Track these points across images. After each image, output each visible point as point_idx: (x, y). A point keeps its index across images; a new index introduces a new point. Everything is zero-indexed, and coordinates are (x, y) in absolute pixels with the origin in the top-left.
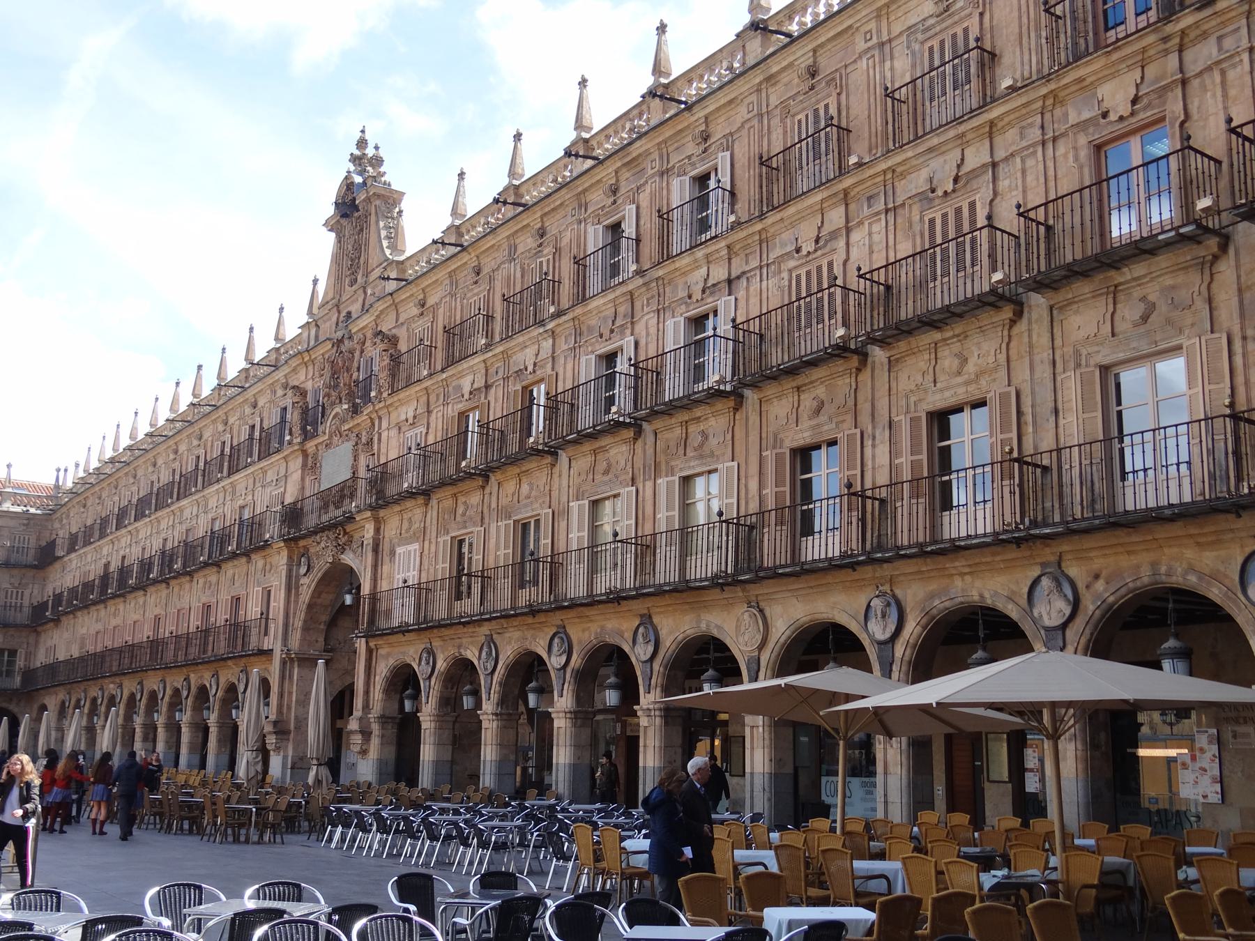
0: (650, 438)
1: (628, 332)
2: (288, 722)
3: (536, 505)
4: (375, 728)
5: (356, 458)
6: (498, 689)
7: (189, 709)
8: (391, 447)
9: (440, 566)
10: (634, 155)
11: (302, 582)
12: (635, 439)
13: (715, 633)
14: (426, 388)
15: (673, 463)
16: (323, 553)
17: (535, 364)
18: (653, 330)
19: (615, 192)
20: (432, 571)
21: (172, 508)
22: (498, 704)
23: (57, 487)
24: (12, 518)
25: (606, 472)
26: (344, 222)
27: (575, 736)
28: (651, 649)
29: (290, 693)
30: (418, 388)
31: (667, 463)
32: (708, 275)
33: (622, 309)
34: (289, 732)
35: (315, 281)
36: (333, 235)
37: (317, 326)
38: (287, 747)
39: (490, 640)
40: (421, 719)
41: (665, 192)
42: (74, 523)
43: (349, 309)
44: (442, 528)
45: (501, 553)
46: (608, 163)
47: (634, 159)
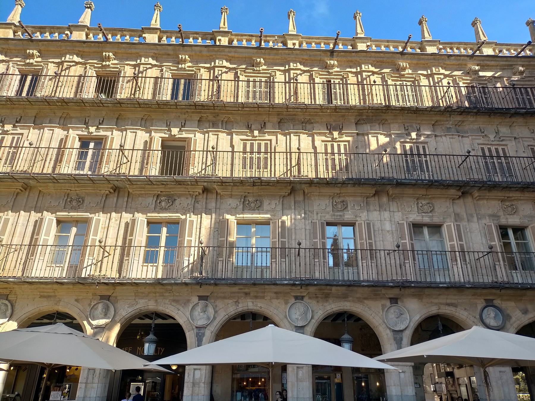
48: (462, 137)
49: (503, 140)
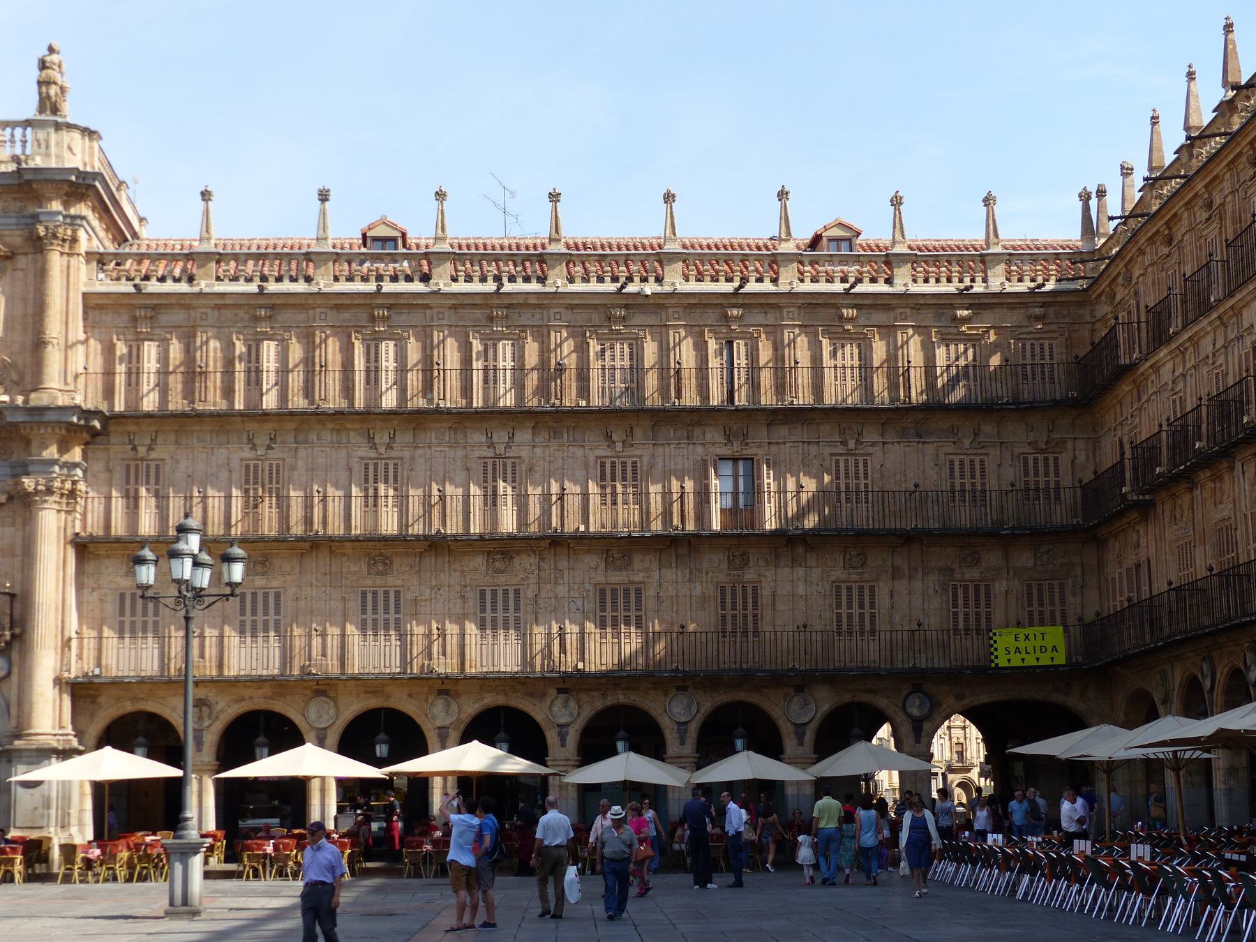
24: (1011, 307)
48: (924, 443)
49: (982, 447)
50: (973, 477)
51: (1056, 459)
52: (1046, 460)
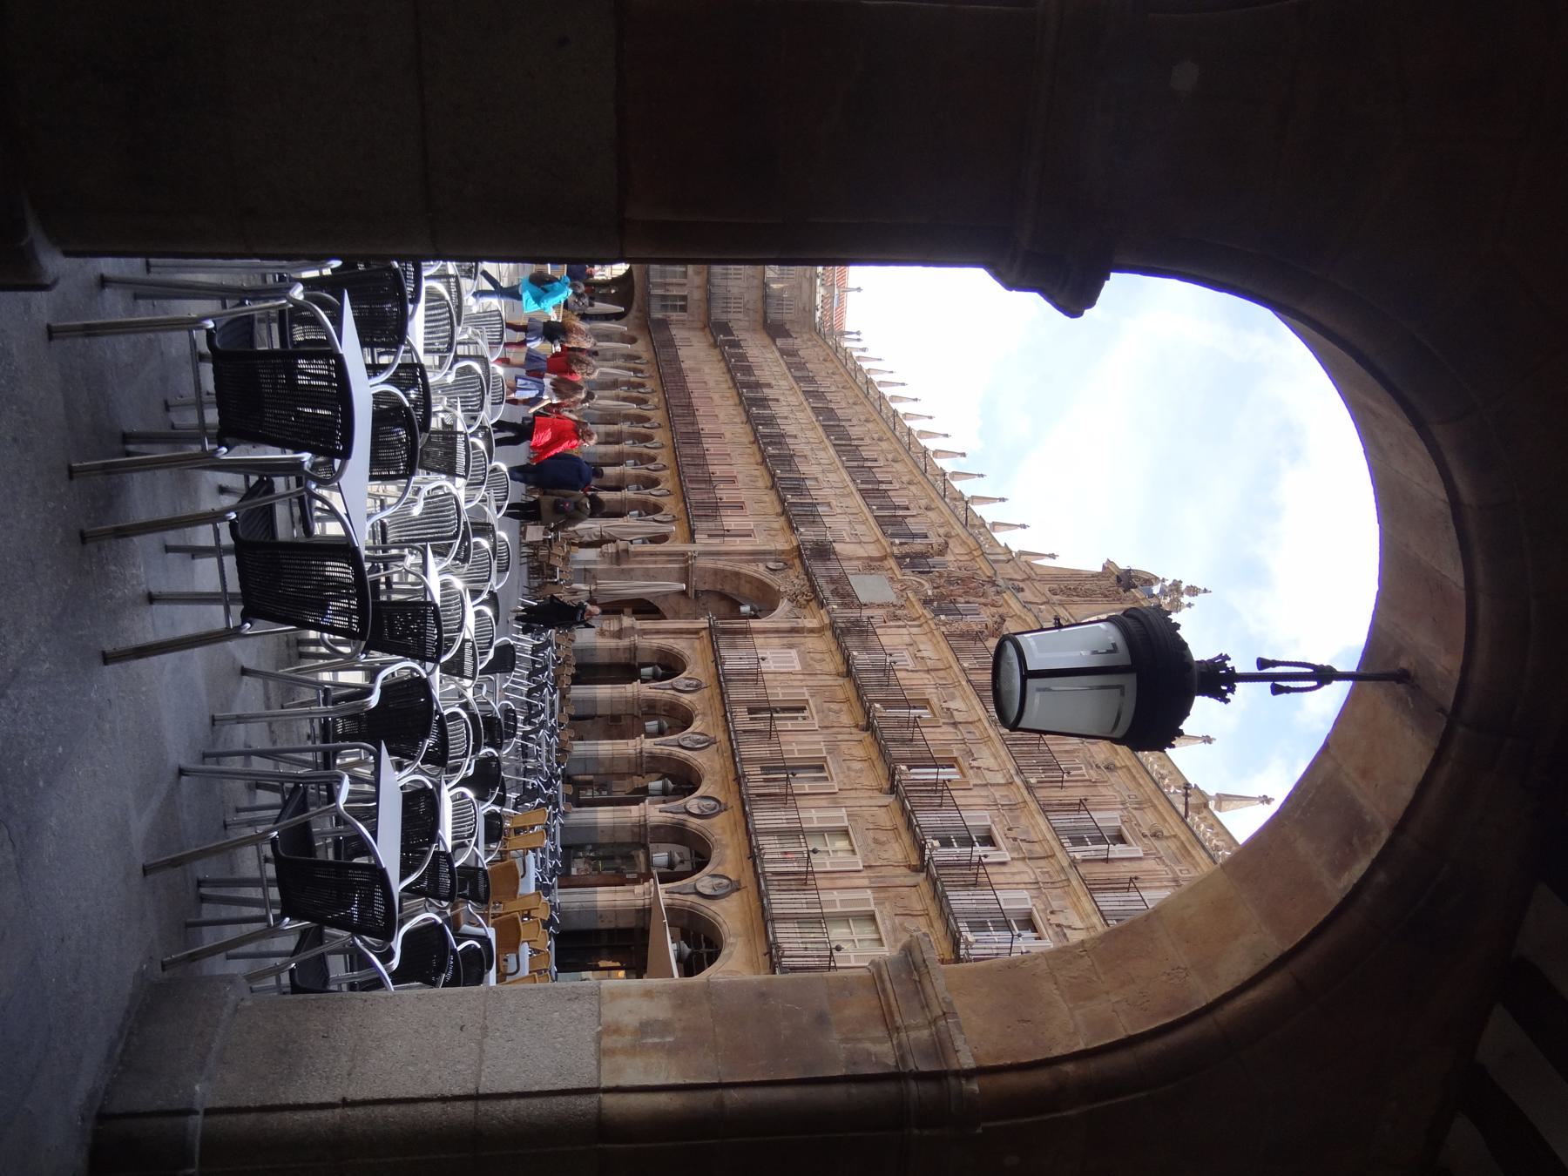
0: (910, 881)
1: (1015, 855)
2: (628, 562)
3: (841, 777)
4: (625, 642)
5: (880, 606)
6: (666, 752)
7: (638, 472)
8: (892, 638)
9: (779, 691)
10: (1193, 852)
11: (760, 565)
12: (909, 867)
13: (725, 952)
14: (951, 667)
15: (887, 904)
16: (788, 582)
17: (979, 768)
18: (1017, 879)
19: (1154, 835)
20: (776, 683)
21: (826, 440)
22: (651, 753)
23: (842, 333)
24: (810, 297)
25: (876, 841)
26: (1113, 578)
27: (623, 827)
28: (708, 891)
29: (655, 562)
30: (950, 659)
31: (887, 898)
32: (1075, 929)
33: (1037, 847)
34: (618, 564)
35: (1053, 556)
36: (1100, 569)
37: (1009, 561)
38: (605, 563)
39: (712, 742)
40: (635, 683)
41: (1158, 884)
42: (808, 351)
43: (1027, 590)
44: (816, 691)
45: (795, 747)
46: (1183, 827)
47: (1189, 853)
50: (735, 274)
51: (740, 312)
52: (740, 308)
